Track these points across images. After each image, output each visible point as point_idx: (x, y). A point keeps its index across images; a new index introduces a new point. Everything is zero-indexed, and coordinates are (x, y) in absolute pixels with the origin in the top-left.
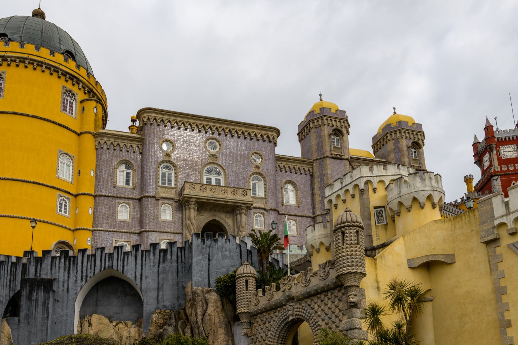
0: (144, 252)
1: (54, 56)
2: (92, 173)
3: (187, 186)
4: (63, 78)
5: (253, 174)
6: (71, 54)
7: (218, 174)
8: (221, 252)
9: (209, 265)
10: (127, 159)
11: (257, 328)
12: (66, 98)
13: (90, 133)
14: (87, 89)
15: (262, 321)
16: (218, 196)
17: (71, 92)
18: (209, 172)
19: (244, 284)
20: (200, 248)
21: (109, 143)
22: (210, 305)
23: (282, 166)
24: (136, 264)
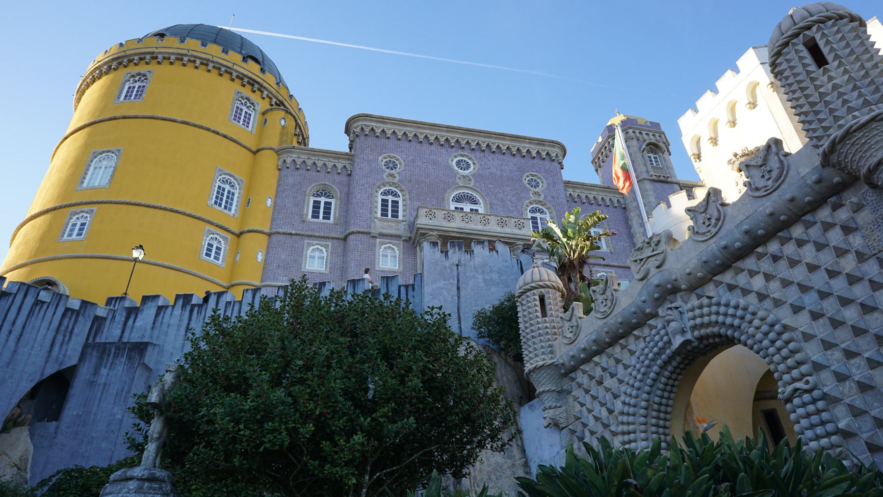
1: (227, 53)
2: (269, 202)
3: (422, 212)
5: (531, 203)
6: (253, 56)
7: (475, 202)
8: (483, 273)
9: (459, 298)
12: (241, 107)
15: (592, 378)
16: (474, 227)
17: (249, 100)
18: (458, 199)
19: (538, 303)
21: (299, 161)
23: (575, 195)
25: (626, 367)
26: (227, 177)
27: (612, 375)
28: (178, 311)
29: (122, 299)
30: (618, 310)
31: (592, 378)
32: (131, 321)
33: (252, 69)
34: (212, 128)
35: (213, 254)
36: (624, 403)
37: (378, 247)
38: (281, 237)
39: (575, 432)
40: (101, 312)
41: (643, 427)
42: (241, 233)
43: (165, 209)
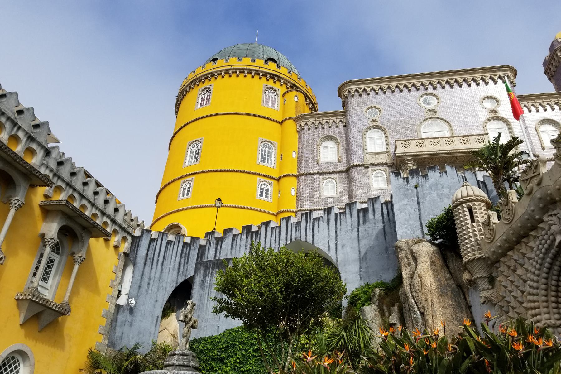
0: (339, 214)
3: (399, 144)
4: (264, 79)
8: (436, 190)
9: (419, 210)
10: (330, 134)
11: (503, 283)
12: (268, 94)
13: (291, 119)
14: (289, 84)
15: (509, 267)
16: (442, 149)
19: (467, 213)
20: (403, 190)
21: (309, 123)
22: (419, 261)
24: (329, 231)
25: (529, 259)
26: (266, 143)
27: (522, 265)
28: (244, 237)
29: (213, 233)
30: (517, 218)
31: (509, 267)
32: (219, 246)
33: (272, 66)
34: (252, 113)
35: (264, 194)
36: (531, 287)
37: (370, 174)
38: (304, 177)
39: (503, 307)
40: (203, 242)
41: (545, 304)
42: (280, 178)
43: (232, 171)
